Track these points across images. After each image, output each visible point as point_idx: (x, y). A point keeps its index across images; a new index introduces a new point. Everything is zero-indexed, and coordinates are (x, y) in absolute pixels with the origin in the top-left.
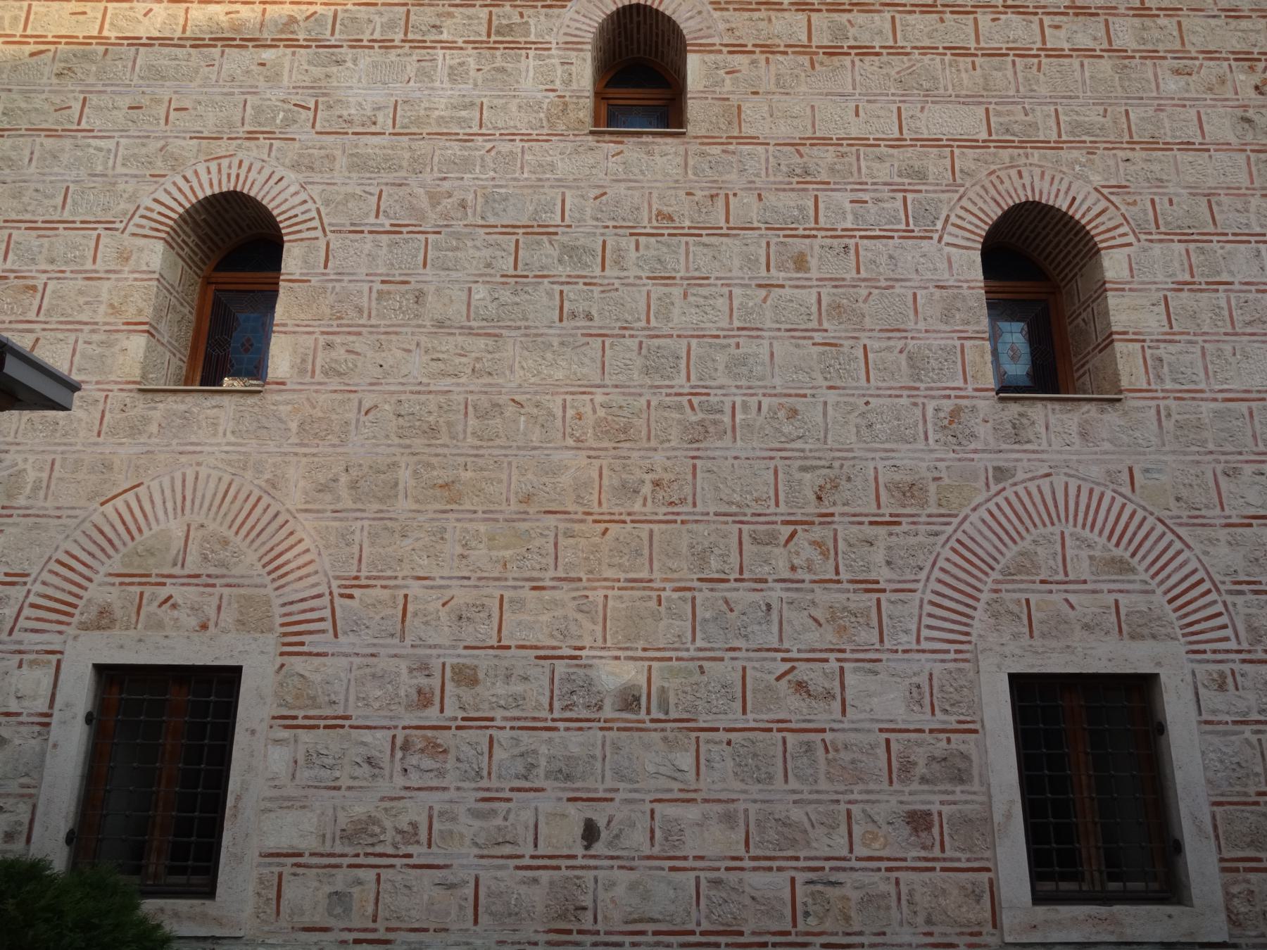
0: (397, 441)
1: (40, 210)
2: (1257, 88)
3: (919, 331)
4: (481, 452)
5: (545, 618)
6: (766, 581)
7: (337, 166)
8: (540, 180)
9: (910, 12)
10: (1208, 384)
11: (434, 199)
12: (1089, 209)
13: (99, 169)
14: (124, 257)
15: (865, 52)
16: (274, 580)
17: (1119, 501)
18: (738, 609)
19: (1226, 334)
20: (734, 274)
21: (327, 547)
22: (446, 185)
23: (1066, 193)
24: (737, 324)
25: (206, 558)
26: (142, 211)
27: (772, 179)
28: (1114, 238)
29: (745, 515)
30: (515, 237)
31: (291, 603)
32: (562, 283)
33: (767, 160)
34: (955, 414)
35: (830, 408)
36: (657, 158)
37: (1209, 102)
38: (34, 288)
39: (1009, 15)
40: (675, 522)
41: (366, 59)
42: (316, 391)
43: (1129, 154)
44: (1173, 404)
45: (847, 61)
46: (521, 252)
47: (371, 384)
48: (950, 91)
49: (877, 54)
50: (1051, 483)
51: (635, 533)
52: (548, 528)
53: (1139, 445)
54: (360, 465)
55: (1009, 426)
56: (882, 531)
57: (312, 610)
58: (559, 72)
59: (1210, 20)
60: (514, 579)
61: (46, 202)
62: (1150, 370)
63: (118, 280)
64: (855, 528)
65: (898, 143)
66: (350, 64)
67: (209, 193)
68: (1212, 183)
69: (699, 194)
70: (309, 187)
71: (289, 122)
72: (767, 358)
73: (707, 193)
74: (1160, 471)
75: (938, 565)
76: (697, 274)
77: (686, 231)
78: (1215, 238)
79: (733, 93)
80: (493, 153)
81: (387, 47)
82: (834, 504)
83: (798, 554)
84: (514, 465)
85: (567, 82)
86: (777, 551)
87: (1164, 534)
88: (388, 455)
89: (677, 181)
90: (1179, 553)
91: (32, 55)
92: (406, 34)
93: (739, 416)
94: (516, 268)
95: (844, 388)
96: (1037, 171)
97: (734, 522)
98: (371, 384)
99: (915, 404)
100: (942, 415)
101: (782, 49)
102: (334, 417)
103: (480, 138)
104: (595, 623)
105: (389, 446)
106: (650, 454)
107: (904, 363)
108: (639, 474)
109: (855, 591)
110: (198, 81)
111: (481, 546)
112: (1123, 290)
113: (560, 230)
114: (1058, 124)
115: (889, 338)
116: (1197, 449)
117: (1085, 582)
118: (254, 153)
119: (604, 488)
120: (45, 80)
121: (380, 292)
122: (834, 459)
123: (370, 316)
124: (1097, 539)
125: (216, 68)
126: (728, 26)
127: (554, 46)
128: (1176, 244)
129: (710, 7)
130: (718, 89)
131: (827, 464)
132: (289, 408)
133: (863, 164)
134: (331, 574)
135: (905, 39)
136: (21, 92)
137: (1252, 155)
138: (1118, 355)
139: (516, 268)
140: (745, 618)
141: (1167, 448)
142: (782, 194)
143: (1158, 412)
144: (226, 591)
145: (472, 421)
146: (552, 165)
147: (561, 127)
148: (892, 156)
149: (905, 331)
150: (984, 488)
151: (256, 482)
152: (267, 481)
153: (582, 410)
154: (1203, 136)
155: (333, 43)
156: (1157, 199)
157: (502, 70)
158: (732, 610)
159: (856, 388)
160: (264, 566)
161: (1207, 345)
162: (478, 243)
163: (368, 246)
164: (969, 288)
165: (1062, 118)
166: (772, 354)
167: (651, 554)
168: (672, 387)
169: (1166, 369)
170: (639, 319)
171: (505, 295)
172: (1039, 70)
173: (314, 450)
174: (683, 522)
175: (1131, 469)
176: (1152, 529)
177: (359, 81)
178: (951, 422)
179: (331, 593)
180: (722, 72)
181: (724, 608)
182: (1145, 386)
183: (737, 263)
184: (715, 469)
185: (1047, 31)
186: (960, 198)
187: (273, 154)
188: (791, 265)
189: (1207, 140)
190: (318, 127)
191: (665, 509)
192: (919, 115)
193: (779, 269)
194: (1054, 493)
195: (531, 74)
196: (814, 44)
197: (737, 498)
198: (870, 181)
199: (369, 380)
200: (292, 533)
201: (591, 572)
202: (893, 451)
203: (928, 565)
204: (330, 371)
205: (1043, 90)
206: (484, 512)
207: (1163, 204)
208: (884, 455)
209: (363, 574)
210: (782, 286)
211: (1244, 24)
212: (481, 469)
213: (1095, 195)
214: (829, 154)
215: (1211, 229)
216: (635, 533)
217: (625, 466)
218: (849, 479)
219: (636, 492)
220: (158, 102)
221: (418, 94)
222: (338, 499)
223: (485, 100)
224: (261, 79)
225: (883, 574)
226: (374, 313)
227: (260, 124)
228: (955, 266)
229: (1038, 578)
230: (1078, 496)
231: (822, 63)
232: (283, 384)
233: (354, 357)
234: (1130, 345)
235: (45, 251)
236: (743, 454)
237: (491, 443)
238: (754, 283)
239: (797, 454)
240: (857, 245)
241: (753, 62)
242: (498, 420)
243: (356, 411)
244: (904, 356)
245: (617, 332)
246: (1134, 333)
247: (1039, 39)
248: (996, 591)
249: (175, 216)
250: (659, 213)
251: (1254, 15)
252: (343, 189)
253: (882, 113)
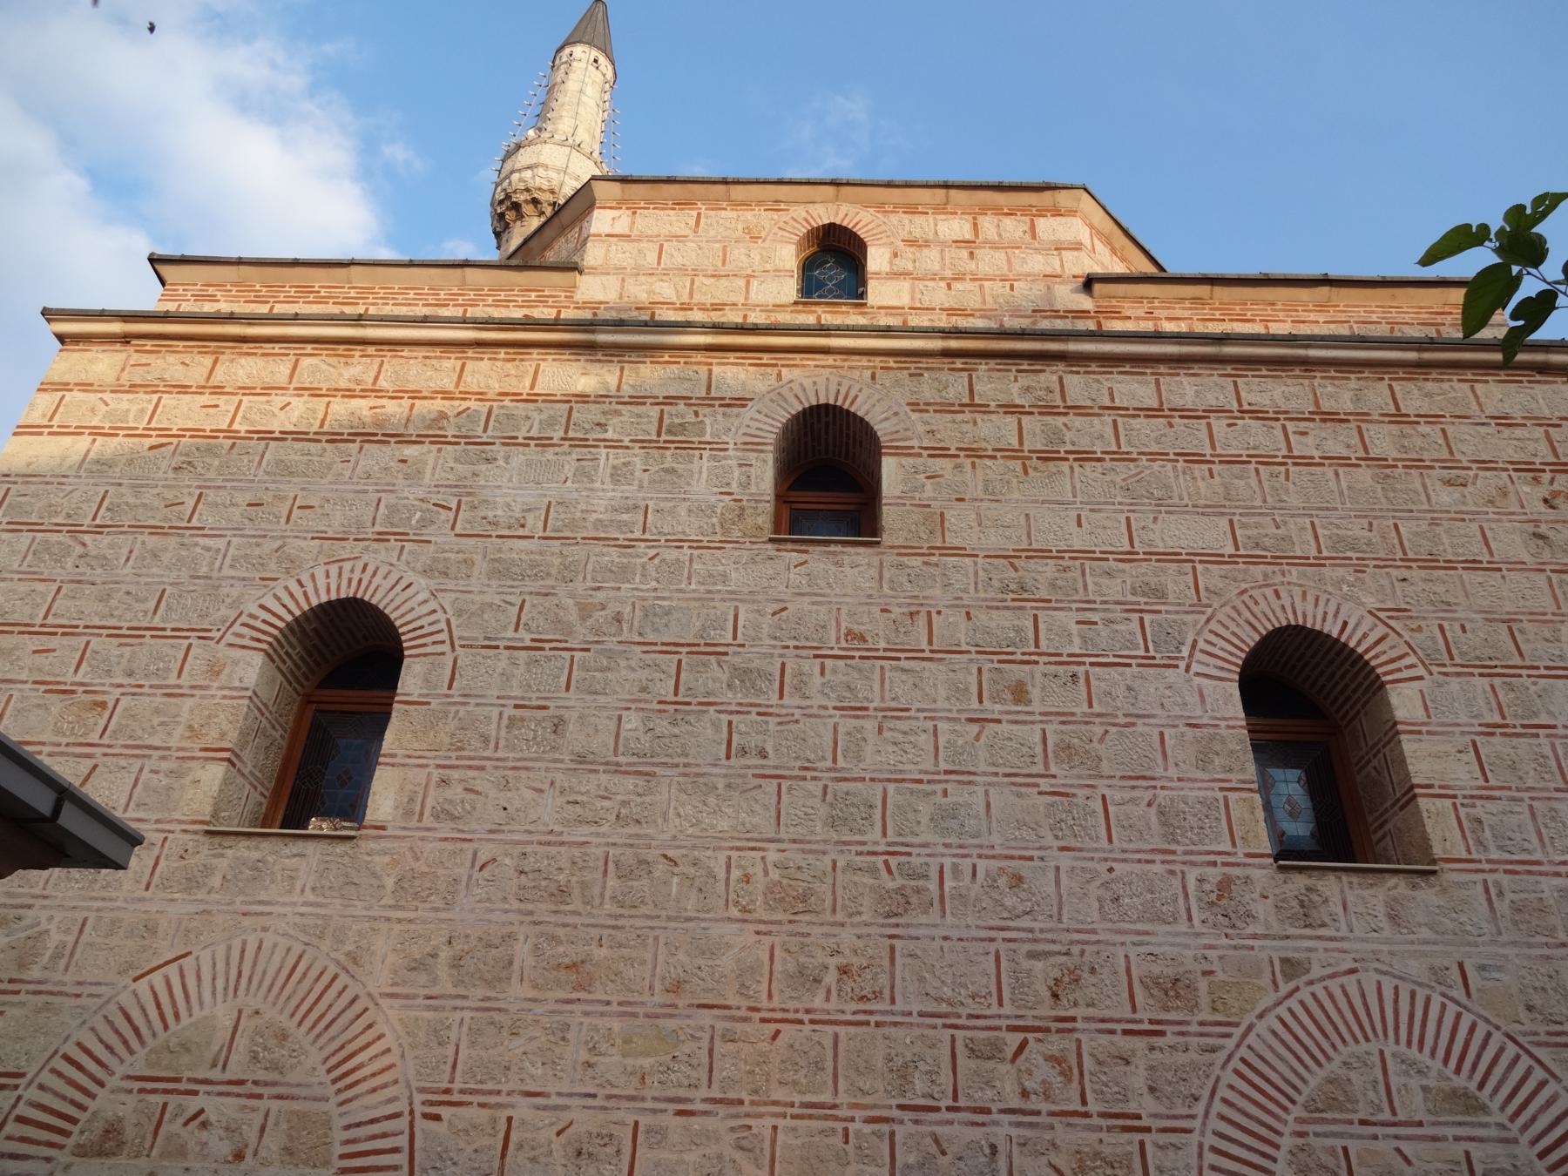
0: (516, 905)
1: (128, 615)
2: (1546, 501)
3: (1171, 780)
4: (621, 922)
5: (693, 1157)
6: (988, 1111)
7: (476, 573)
8: (710, 592)
9: (1134, 416)
10: (1546, 854)
11: (585, 611)
12: (1365, 636)
13: (204, 570)
14: (215, 670)
15: (1084, 457)
16: (339, 1091)
17: (1452, 1009)
18: (952, 1150)
19: (1558, 790)
20: (941, 704)
21: (413, 1047)
22: (600, 596)
23: (1336, 615)
24: (943, 766)
25: (255, 1058)
26: (244, 619)
27: (982, 595)
28: (1399, 670)
29: (959, 1017)
30: (677, 657)
31: (358, 1125)
32: (731, 713)
33: (976, 573)
34: (1225, 885)
35: (1063, 876)
36: (847, 569)
37: (1492, 516)
38: (103, 705)
39: (1247, 421)
40: (868, 1023)
41: (519, 457)
42: (422, 839)
43: (1405, 573)
44: (1505, 880)
45: (1065, 466)
46: (683, 675)
47: (491, 832)
48: (1186, 501)
49: (1099, 460)
50: (1359, 983)
51: (816, 1037)
52: (702, 1028)
53: (1469, 933)
54: (467, 936)
55: (1295, 903)
56: (1140, 1043)
57: (384, 1135)
58: (736, 474)
59: (1479, 428)
60: (655, 1099)
61: (137, 606)
62: (1468, 834)
63: (202, 697)
64: (1104, 1039)
65: (1129, 557)
66: (501, 462)
67: (324, 599)
68: (1509, 607)
69: (897, 611)
70: (440, 595)
71: (425, 523)
72: (982, 810)
73: (905, 610)
74: (1499, 969)
75: (1219, 1094)
76: (894, 705)
77: (881, 654)
78: (1524, 672)
79: (935, 499)
80: (656, 561)
81: (544, 445)
82: (1076, 1004)
83: (1030, 1073)
84: (662, 941)
85: (745, 485)
86: (1004, 1068)
87: (1517, 1058)
88: (504, 924)
89: (870, 596)
90: (1542, 1084)
91: (151, 448)
92: (566, 432)
93: (948, 884)
94: (676, 694)
95: (1080, 850)
96: (1297, 591)
97: (945, 1026)
98: (491, 832)
99: (1172, 873)
100: (1207, 887)
101: (990, 453)
102: (441, 872)
103: (642, 544)
104: (759, 1167)
105: (506, 911)
106: (836, 930)
107: (1154, 820)
108: (821, 957)
109: (1109, 1129)
110: (330, 478)
111: (614, 1050)
112: (1419, 732)
113: (731, 650)
114: (1316, 538)
115: (1133, 788)
116: (1544, 940)
117: (1420, 1124)
118: (382, 556)
119: (776, 975)
120: (160, 474)
121: (511, 719)
122: (1072, 942)
123: (497, 748)
124: (1429, 1062)
125: (351, 465)
126: (928, 428)
127: (731, 446)
128: (1477, 678)
129: (907, 408)
130: (917, 495)
131: (1064, 950)
132: (387, 859)
133: (1089, 579)
134: (414, 1084)
135: (1130, 443)
136: (133, 486)
137: (1554, 577)
138: (1425, 815)
139: (676, 694)
140: (961, 1164)
141: (1504, 938)
142: (994, 613)
143: (1487, 890)
144: (275, 1105)
145: (612, 882)
146: (724, 575)
147: (736, 534)
148: (1123, 571)
149: (1153, 779)
150: (1271, 988)
151: (333, 955)
152: (348, 954)
153: (750, 870)
154: (1492, 555)
155: (484, 440)
156: (1446, 625)
157: (673, 471)
158: (944, 1153)
159: (1096, 850)
160: (329, 1071)
161: (1535, 804)
162: (633, 663)
163: (502, 665)
164: (1228, 727)
165: (1320, 531)
166: (988, 805)
167: (835, 1068)
168: (863, 843)
169: (1488, 833)
170: (824, 758)
171: (662, 726)
172: (1287, 479)
173: (411, 915)
174: (878, 1024)
175: (1461, 965)
176: (1502, 1050)
177: (510, 480)
178: (1220, 897)
179: (412, 1112)
180: (922, 476)
181: (934, 1149)
182: (1464, 855)
183: (942, 692)
184: (919, 953)
185: (1292, 437)
186: (1209, 620)
187: (403, 558)
188: (1008, 696)
189: (1497, 558)
190: (458, 529)
191: (855, 1006)
192: (1152, 526)
193: (993, 699)
194: (1363, 996)
195: (705, 475)
196: (1026, 448)
197: (947, 992)
198: (1098, 599)
199: (488, 827)
200: (370, 1026)
201: (756, 1092)
202: (1147, 933)
203: (1206, 1094)
204: (443, 814)
205: (1294, 501)
206: (620, 1004)
207: (1453, 632)
208: (1137, 938)
209: (457, 1086)
210: (999, 721)
211: (1518, 432)
212: (620, 945)
213: (1370, 620)
214: (1049, 569)
215: (1517, 661)
216: (816, 1037)
217: (803, 946)
218: (1093, 971)
219: (817, 981)
220: (282, 498)
221: (575, 495)
222: (435, 981)
223: (651, 503)
224: (400, 476)
225: (1146, 1106)
226: (502, 743)
227: (392, 525)
228: (1208, 700)
229: (1356, 1117)
230: (1396, 1001)
231: (1036, 469)
232: (383, 828)
233: (473, 796)
234: (1438, 801)
235: (124, 661)
236: (955, 934)
237: (633, 912)
238: (963, 716)
239: (1023, 935)
240: (1087, 673)
241: (957, 467)
242: (645, 882)
243: (468, 864)
244: (1153, 811)
245: (796, 772)
246: (1441, 787)
247: (1283, 445)
248: (1301, 1135)
249: (281, 624)
250: (849, 632)
251: (1528, 423)
252: (478, 598)
253: (1108, 523)
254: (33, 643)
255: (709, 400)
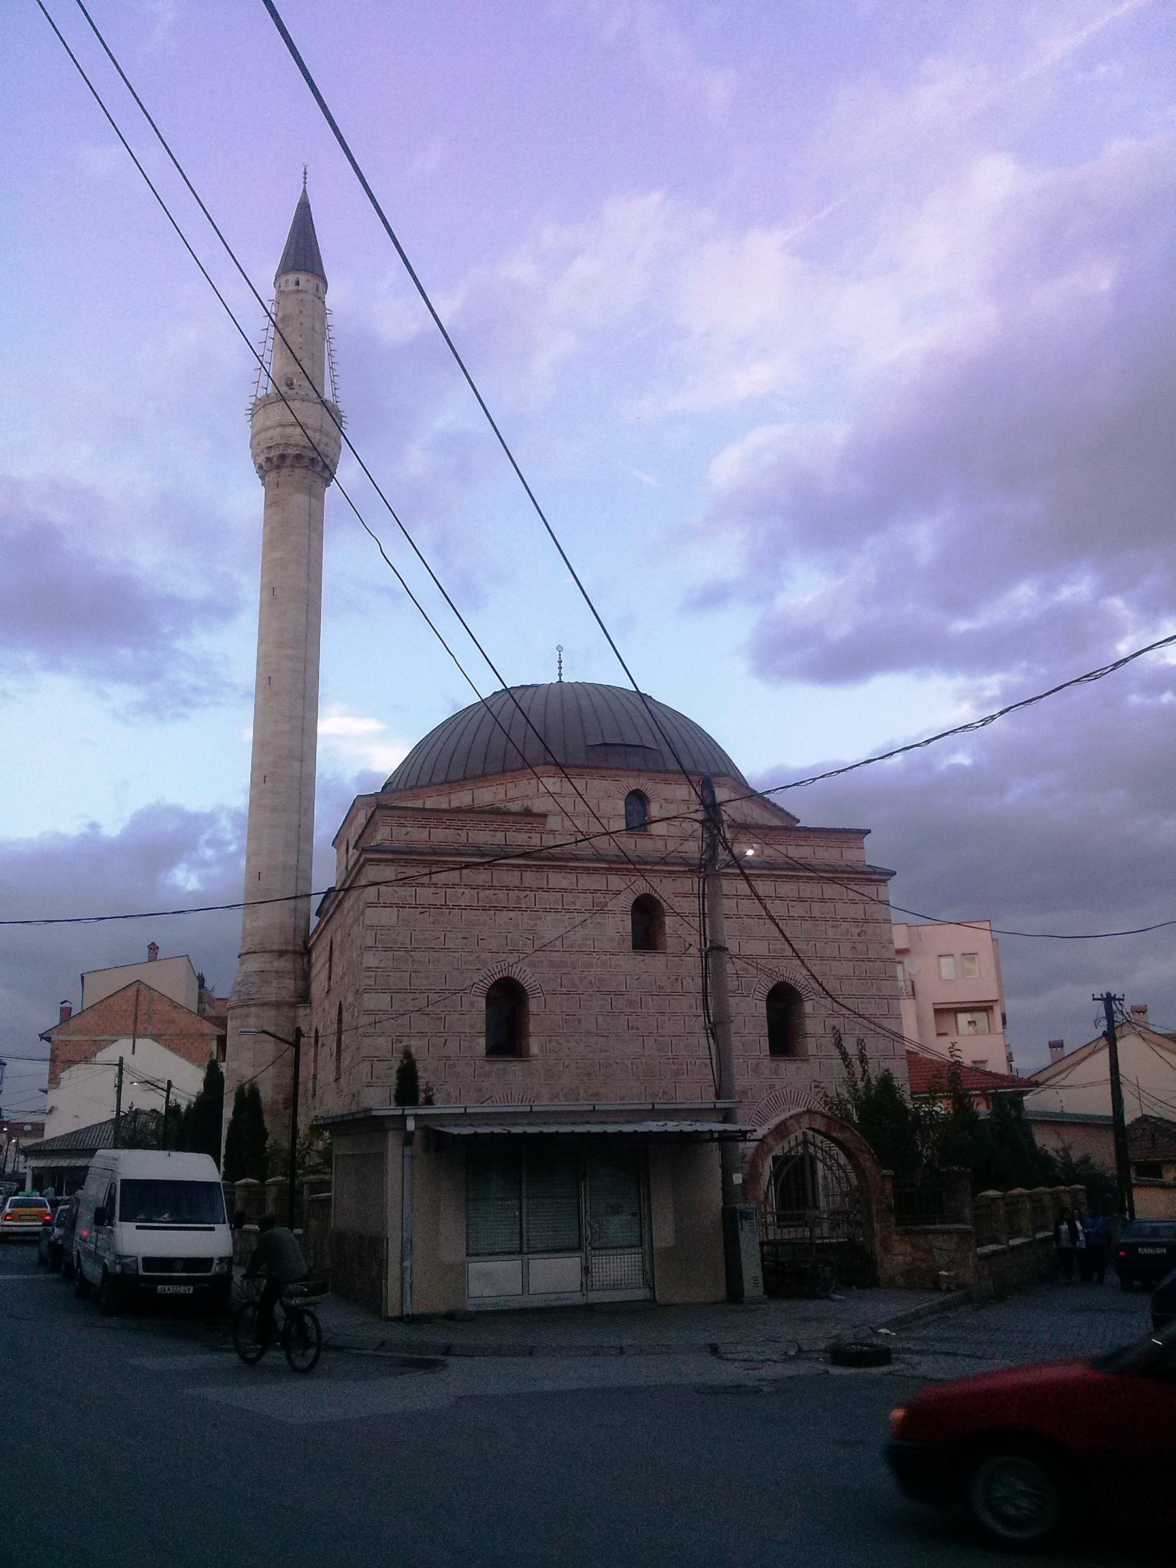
14: (472, 1004)
34: (757, 1065)
41: (551, 916)
71: (525, 945)
254: (411, 996)
255: (607, 892)
